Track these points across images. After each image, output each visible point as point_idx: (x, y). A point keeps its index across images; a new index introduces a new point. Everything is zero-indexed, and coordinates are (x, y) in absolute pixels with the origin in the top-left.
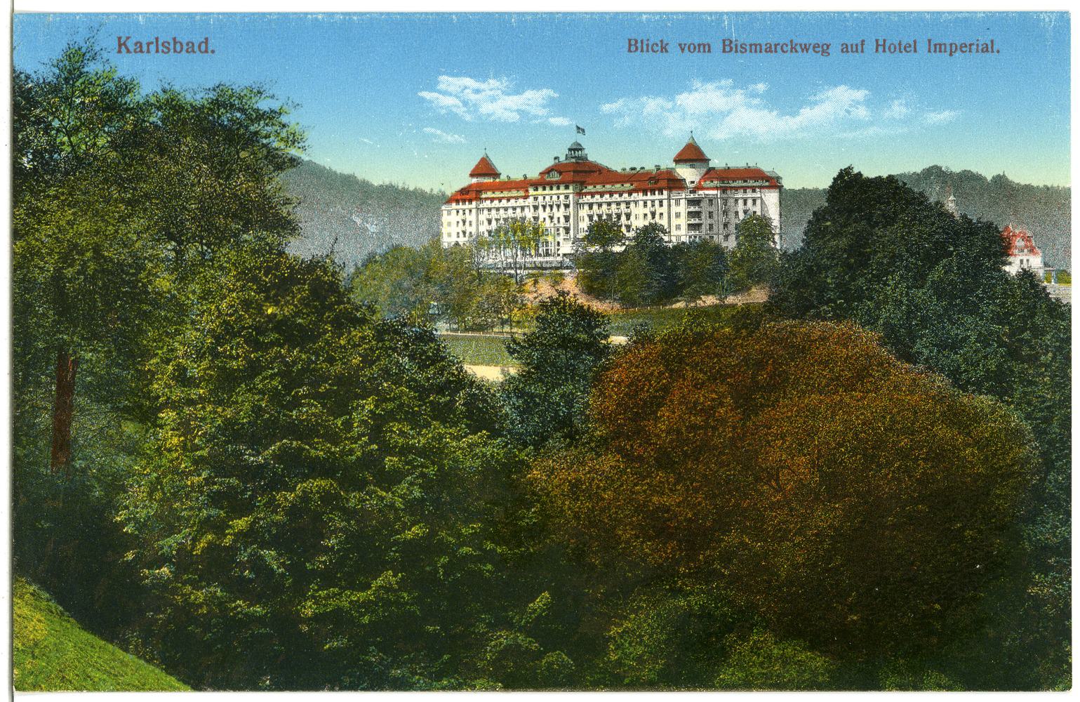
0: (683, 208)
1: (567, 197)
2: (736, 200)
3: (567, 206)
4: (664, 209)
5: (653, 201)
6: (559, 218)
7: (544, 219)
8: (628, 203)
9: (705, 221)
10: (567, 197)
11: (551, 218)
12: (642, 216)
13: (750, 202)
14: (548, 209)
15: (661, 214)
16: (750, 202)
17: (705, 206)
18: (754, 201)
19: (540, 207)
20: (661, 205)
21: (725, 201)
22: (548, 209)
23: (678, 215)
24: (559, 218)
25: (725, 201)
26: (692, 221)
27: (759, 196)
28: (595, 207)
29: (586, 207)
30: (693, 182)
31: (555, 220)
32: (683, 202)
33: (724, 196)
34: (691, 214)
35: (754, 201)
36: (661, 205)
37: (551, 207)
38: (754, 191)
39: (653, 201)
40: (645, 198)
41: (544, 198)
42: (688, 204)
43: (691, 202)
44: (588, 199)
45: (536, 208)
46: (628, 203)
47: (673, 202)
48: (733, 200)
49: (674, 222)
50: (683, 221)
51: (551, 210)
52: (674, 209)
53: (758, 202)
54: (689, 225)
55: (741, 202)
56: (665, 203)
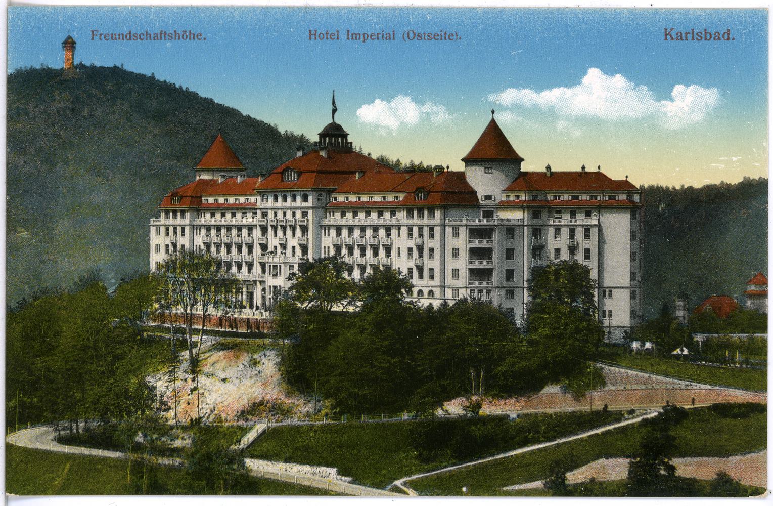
0: (462, 242)
1: (305, 214)
2: (558, 230)
3: (304, 229)
4: (435, 243)
5: (421, 229)
6: (294, 248)
7: (275, 247)
8: (388, 229)
9: (497, 261)
10: (305, 214)
11: (284, 247)
12: (404, 253)
13: (580, 233)
14: (280, 233)
15: (432, 250)
16: (580, 233)
17: (497, 242)
19: (270, 229)
20: (432, 236)
21: (537, 232)
22: (280, 233)
23: (456, 253)
24: (294, 248)
25: (537, 232)
26: (477, 265)
27: (595, 222)
28: (345, 232)
29: (333, 232)
30: (488, 198)
31: (289, 251)
32: (463, 233)
33: (535, 221)
34: (476, 253)
36: (432, 236)
38: (588, 214)
39: (421, 229)
40: (410, 222)
41: (276, 214)
42: (470, 237)
43: (476, 232)
44: (335, 218)
45: (264, 229)
46: (388, 229)
47: (449, 230)
48: (551, 231)
49: (451, 264)
50: (463, 264)
51: (285, 234)
52: (451, 243)
53: (594, 232)
54: (472, 271)
55: (565, 233)
56: (437, 230)
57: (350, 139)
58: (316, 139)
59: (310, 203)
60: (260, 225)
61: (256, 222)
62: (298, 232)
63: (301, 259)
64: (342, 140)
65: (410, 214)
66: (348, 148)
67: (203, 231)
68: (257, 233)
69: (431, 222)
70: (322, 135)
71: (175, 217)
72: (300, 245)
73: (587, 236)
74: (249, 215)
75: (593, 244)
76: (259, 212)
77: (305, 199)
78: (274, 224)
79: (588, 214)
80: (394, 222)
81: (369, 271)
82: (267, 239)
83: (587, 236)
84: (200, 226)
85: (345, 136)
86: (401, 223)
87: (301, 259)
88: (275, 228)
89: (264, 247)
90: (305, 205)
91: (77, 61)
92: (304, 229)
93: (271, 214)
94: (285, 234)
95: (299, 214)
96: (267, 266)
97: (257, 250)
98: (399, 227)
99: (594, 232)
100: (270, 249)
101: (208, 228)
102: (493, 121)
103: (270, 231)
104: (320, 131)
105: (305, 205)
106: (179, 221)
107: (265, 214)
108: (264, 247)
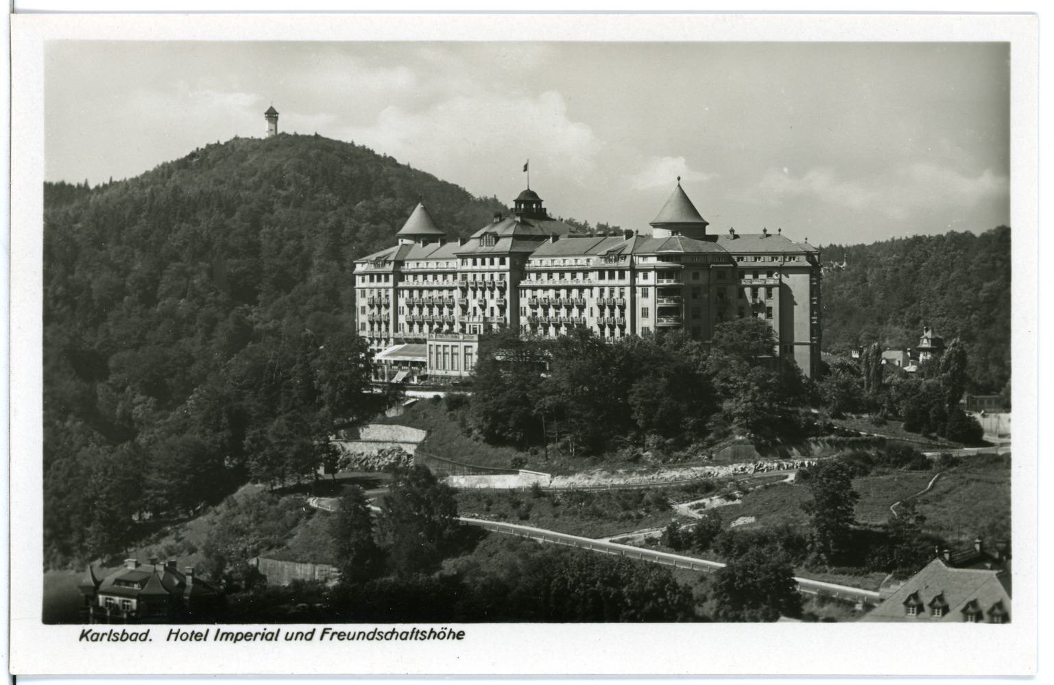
3: (502, 290)
6: (492, 309)
10: (502, 277)
11: (483, 307)
13: (762, 292)
14: (479, 293)
16: (762, 292)
18: (769, 289)
22: (479, 293)
23: (645, 313)
24: (492, 309)
35: (769, 289)
37: (483, 290)
38: (770, 275)
40: (602, 282)
45: (464, 291)
51: (483, 295)
53: (775, 291)
57: (544, 206)
58: (511, 205)
59: (507, 266)
60: (461, 288)
61: (456, 284)
62: (497, 293)
63: (499, 319)
64: (537, 206)
65: (602, 277)
66: (542, 215)
67: (406, 293)
68: (457, 294)
69: (622, 282)
70: (518, 202)
71: (379, 280)
72: (498, 306)
73: (769, 295)
74: (450, 277)
75: (774, 303)
76: (459, 275)
77: (502, 262)
78: (474, 286)
79: (770, 275)
80: (587, 283)
81: (563, 330)
82: (467, 301)
83: (769, 295)
84: (403, 289)
85: (539, 202)
86: (593, 284)
87: (499, 319)
88: (474, 290)
89: (464, 308)
90: (502, 267)
91: (279, 131)
92: (502, 290)
93: (470, 277)
94: (483, 295)
95: (496, 276)
96: (467, 326)
97: (457, 311)
98: (591, 288)
99: (775, 291)
100: (470, 310)
101: (411, 290)
102: (679, 186)
103: (470, 293)
104: (516, 198)
105: (502, 267)
106: (382, 284)
107: (464, 277)
108: (464, 308)
